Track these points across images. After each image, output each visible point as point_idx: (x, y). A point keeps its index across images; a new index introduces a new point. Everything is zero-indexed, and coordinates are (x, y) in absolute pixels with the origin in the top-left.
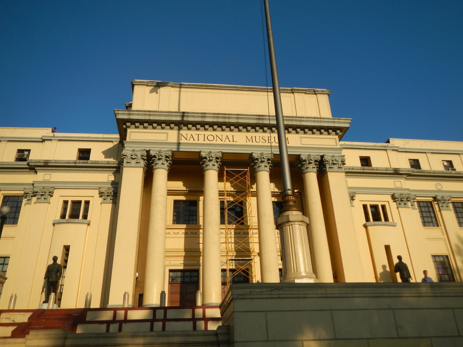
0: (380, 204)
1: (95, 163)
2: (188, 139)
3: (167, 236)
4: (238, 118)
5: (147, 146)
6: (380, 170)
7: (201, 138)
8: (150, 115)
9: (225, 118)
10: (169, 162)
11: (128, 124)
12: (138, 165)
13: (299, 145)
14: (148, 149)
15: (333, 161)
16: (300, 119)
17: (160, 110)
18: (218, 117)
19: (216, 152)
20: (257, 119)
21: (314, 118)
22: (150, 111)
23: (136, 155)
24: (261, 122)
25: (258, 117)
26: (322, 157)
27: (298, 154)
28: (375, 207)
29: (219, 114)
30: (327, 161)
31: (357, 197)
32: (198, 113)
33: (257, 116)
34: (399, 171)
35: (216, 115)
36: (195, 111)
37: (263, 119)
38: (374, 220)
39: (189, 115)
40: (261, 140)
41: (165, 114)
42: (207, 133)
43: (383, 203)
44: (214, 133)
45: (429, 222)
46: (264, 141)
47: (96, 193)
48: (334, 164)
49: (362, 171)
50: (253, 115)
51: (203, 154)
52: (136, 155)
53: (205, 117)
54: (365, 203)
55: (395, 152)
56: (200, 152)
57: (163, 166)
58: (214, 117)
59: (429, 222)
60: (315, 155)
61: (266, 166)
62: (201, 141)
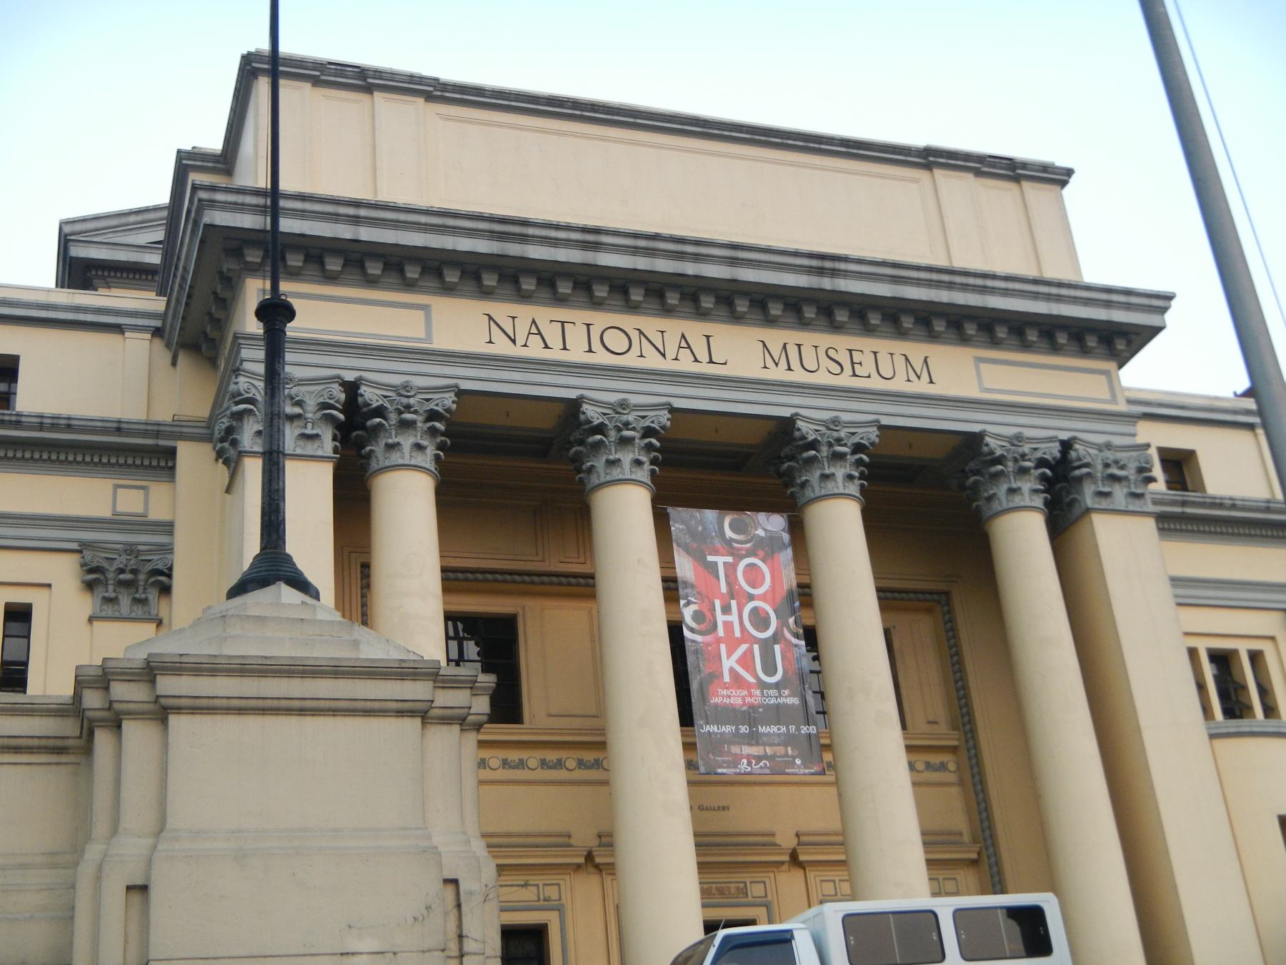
0: (1243, 647)
1: (54, 427)
2: (520, 341)
4: (733, 262)
5: (342, 361)
6: (1244, 509)
7: (576, 337)
8: (356, 221)
9: (680, 256)
10: (440, 439)
11: (254, 256)
12: (310, 448)
13: (975, 393)
14: (350, 376)
15: (1107, 466)
16: (979, 282)
17: (384, 196)
18: (651, 253)
19: (862, 421)
20: (810, 271)
22: (357, 204)
23: (299, 403)
24: (827, 283)
25: (814, 263)
26: (1066, 445)
27: (976, 428)
28: (1223, 660)
30: (1087, 465)
32: (568, 228)
33: (811, 255)
35: (642, 243)
37: (834, 273)
38: (1229, 713)
39: (531, 231)
40: (825, 362)
41: (423, 219)
42: (601, 319)
43: (1256, 645)
44: (630, 322)
46: (837, 369)
47: (62, 572)
48: (1115, 479)
49: (1178, 509)
50: (796, 254)
51: (591, 413)
52: (299, 403)
53: (596, 247)
56: (574, 406)
57: (419, 459)
58: (635, 251)
60: (1043, 435)
61: (638, 463)
62: (577, 354)
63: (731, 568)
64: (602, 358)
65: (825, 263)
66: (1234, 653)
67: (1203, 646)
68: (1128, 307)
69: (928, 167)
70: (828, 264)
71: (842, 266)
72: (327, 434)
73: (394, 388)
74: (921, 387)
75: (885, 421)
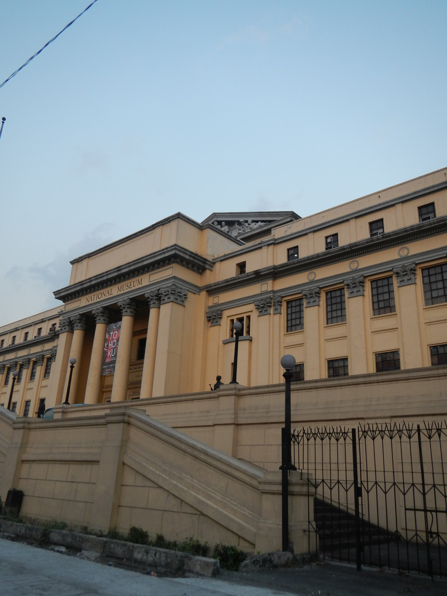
0: (245, 316)
3: (131, 371)
4: (107, 275)
7: (96, 296)
21: (150, 255)
24: (120, 273)
28: (241, 320)
29: (97, 276)
31: (226, 313)
34: (260, 273)
36: (107, 270)
37: (120, 270)
43: (248, 314)
44: (101, 291)
45: (296, 325)
49: (227, 284)
54: (232, 318)
55: (271, 247)
56: (91, 311)
59: (296, 325)
63: (113, 334)
64: (98, 300)
65: (119, 268)
66: (243, 317)
67: (235, 318)
68: (168, 252)
69: (154, 229)
70: (119, 269)
71: (121, 268)
72: (67, 327)
73: (74, 316)
74: (140, 286)
75: (131, 297)
